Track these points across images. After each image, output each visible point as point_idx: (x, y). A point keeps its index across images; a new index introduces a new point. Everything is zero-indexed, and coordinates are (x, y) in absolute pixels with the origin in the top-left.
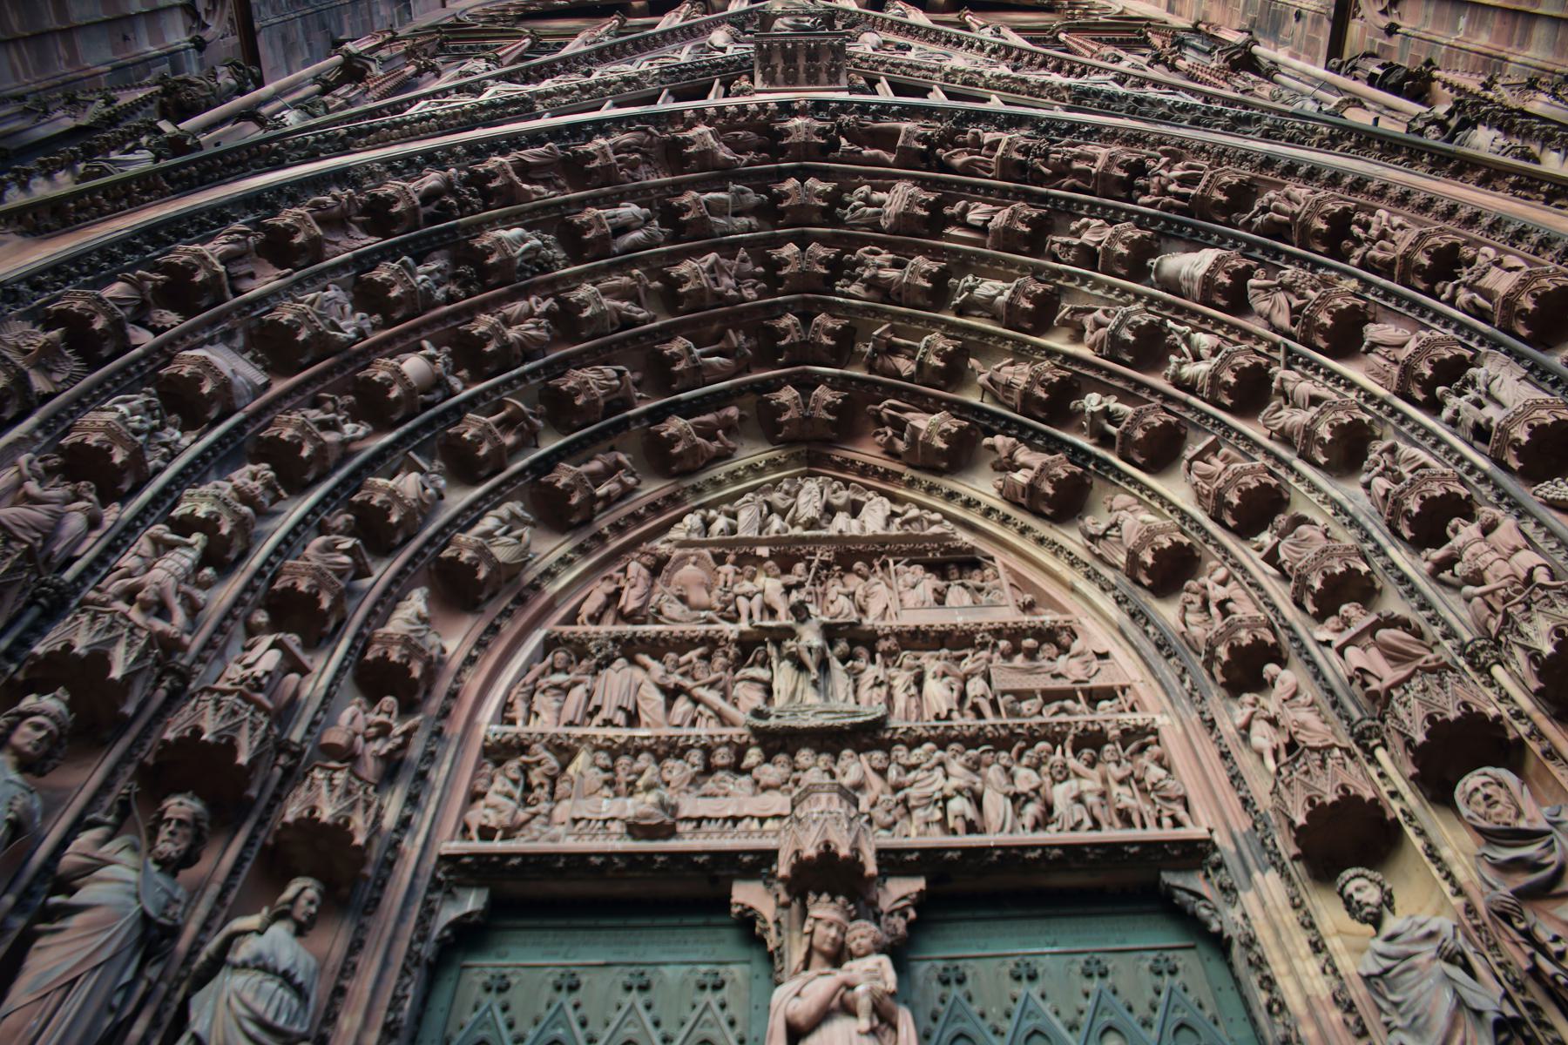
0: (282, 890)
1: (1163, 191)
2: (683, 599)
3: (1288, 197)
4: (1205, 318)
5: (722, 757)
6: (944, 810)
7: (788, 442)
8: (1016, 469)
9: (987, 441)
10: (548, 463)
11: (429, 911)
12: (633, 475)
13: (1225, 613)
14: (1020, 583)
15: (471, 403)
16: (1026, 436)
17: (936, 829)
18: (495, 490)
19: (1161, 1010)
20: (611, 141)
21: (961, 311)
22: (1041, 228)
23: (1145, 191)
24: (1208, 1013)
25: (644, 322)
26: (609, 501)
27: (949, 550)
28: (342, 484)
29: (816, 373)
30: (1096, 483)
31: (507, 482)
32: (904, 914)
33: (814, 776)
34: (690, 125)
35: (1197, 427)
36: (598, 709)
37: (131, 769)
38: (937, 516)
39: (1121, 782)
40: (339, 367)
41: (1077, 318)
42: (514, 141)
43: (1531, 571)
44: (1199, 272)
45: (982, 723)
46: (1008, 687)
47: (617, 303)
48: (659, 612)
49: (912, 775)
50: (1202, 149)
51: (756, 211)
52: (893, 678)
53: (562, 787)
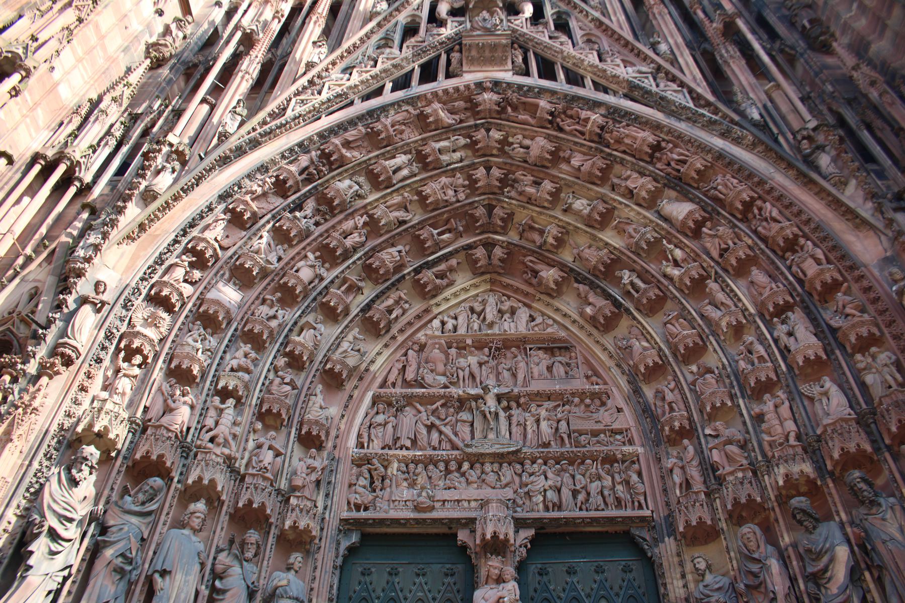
0: (289, 558)
1: (669, 164)
2: (432, 371)
3: (726, 186)
4: (681, 242)
5: (453, 466)
6: (545, 496)
7: (483, 274)
8: (590, 304)
9: (576, 285)
10: (368, 307)
11: (338, 543)
12: (406, 302)
13: (672, 409)
14: (587, 363)
15: (332, 282)
16: (593, 286)
17: (541, 506)
18: (347, 326)
19: (624, 589)
20: (389, 120)
21: (565, 211)
22: (606, 172)
23: (659, 160)
24: (641, 591)
25: (410, 220)
26: (397, 318)
27: (555, 340)
28: (282, 344)
29: (494, 239)
30: (625, 316)
31: (351, 321)
32: (526, 546)
33: (491, 478)
34: (429, 103)
35: (672, 299)
36: (398, 438)
37: (227, 518)
38: (550, 322)
39: (621, 483)
40: (273, 280)
41: (621, 225)
42: (342, 127)
43: (789, 433)
44: (681, 218)
45: (563, 450)
46: (576, 428)
47: (396, 214)
48: (423, 379)
49: (532, 478)
50: (689, 141)
51: (465, 146)
52: (526, 420)
53: (387, 481)
